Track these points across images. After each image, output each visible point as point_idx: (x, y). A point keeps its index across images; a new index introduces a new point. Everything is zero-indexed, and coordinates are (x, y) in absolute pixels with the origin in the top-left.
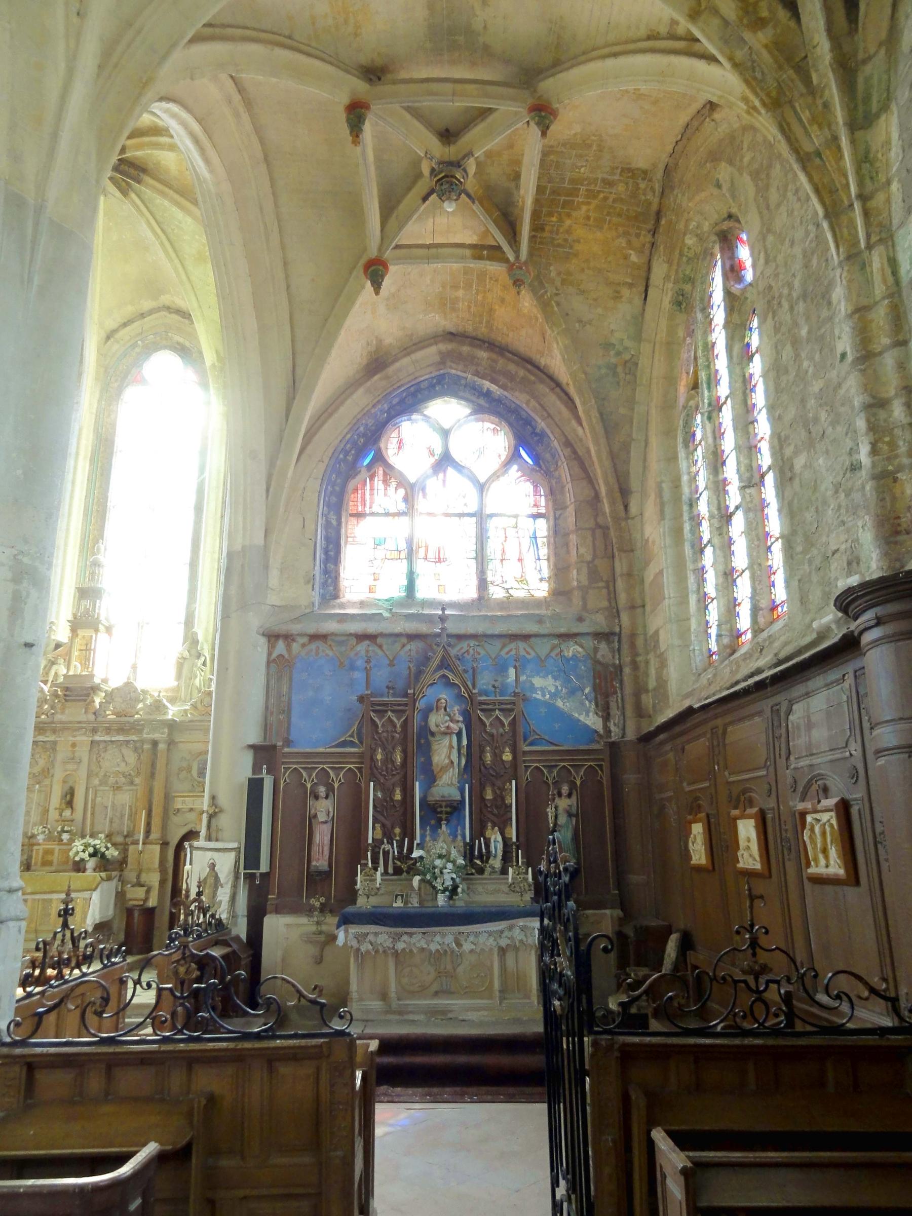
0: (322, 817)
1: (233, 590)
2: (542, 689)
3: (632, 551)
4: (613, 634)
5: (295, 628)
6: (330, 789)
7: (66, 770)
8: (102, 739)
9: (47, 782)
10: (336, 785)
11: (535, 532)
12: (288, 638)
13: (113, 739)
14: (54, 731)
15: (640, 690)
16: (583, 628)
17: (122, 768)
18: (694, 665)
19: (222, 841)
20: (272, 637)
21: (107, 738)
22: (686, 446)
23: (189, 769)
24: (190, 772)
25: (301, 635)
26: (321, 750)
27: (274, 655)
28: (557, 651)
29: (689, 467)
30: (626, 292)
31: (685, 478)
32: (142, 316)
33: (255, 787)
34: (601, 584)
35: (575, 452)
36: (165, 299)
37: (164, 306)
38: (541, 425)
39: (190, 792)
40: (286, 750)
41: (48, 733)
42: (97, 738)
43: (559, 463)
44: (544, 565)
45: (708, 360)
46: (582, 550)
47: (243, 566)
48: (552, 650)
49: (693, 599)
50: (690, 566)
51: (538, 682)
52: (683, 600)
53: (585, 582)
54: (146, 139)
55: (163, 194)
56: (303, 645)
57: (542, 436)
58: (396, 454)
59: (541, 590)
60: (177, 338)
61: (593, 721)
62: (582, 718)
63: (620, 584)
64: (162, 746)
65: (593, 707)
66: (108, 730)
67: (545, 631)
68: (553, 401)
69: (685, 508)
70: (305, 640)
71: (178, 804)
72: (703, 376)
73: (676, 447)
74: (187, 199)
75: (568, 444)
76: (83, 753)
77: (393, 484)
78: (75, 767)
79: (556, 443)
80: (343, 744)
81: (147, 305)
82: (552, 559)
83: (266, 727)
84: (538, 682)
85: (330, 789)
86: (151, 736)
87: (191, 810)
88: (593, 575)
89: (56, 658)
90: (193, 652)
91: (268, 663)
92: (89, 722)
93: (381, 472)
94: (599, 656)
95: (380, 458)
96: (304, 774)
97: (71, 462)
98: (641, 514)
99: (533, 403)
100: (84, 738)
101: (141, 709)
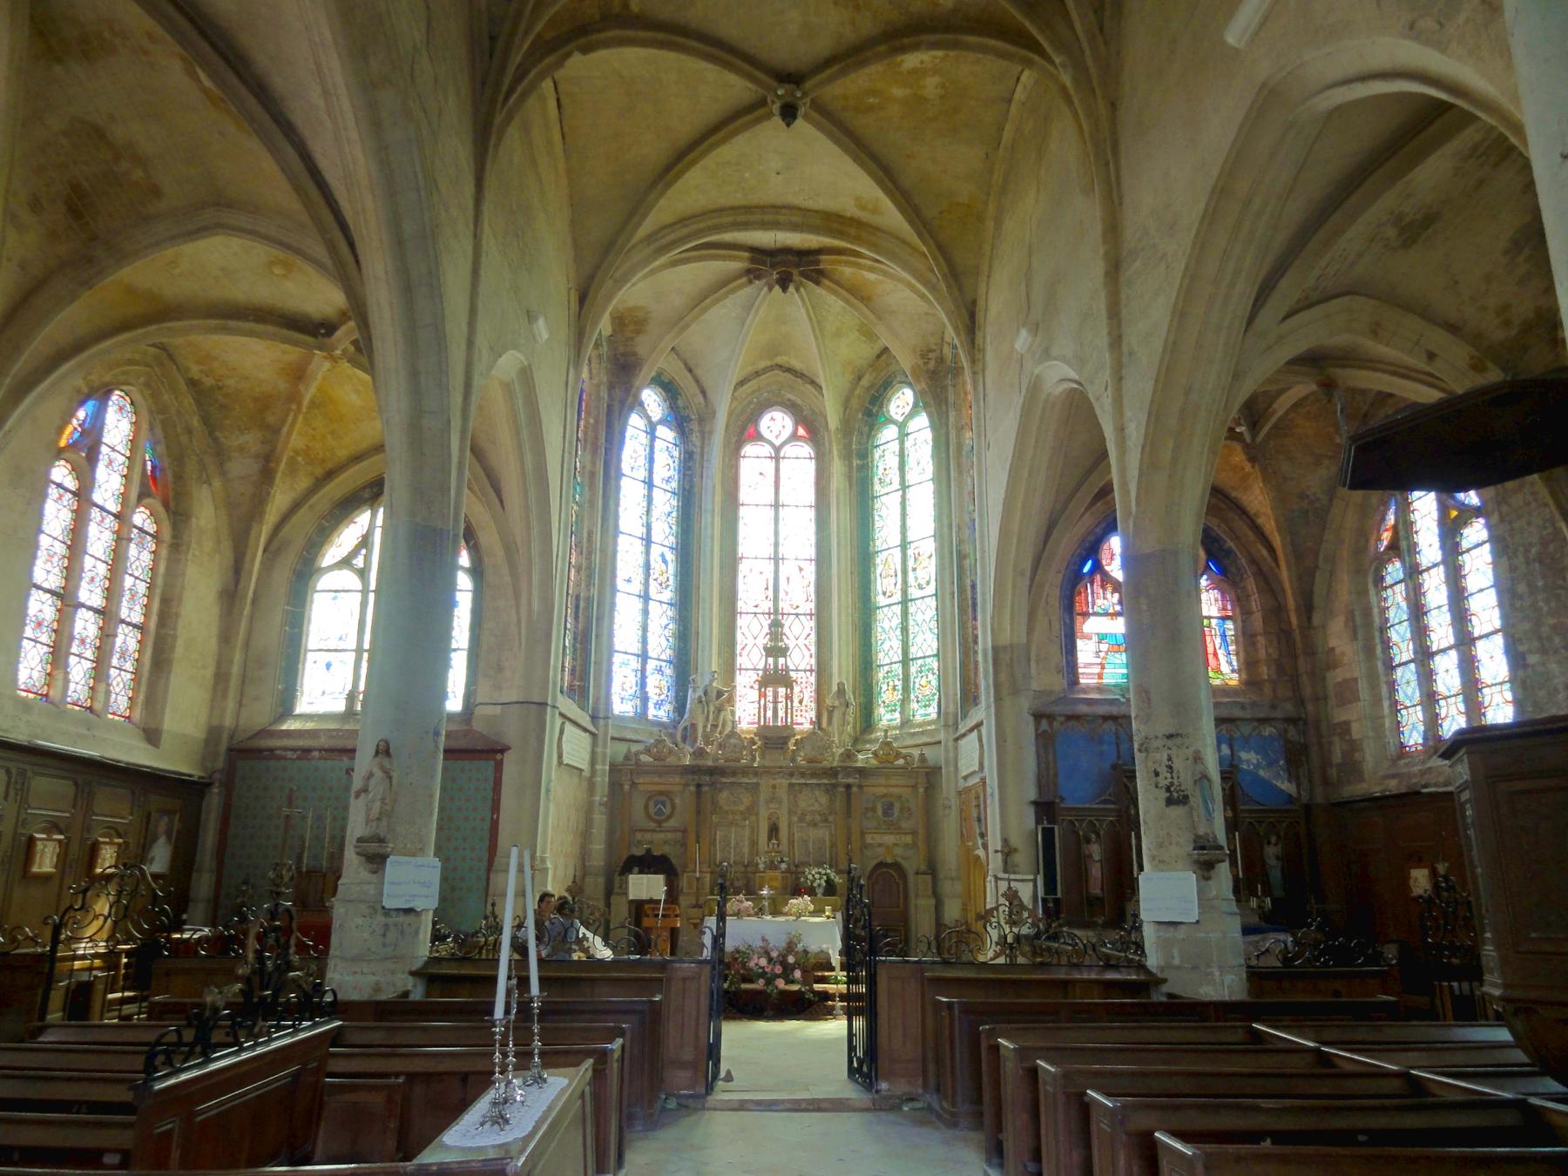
0: (1097, 857)
1: (1003, 676)
2: (1248, 761)
3: (1314, 654)
4: (1300, 719)
5: (1057, 709)
6: (1098, 835)
7: (769, 809)
9: (753, 818)
10: (1102, 833)
11: (1224, 631)
12: (1051, 717)
14: (756, 774)
15: (1326, 764)
16: (1278, 714)
17: (817, 807)
18: (1388, 753)
19: (1019, 873)
20: (1038, 717)
21: (802, 781)
22: (1376, 586)
23: (874, 810)
24: (875, 812)
25: (1060, 715)
26: (1087, 806)
27: (1040, 731)
28: (1257, 731)
29: (1379, 602)
30: (1326, 462)
31: (1376, 610)
32: (757, 374)
33: (1048, 835)
34: (1286, 678)
35: (1260, 569)
36: (779, 360)
37: (777, 365)
38: (1231, 544)
39: (876, 828)
40: (1062, 805)
41: (751, 776)
42: (794, 781)
43: (1245, 576)
44: (1234, 658)
45: (1407, 532)
46: (1270, 650)
47: (1011, 659)
48: (1254, 729)
49: (1386, 704)
50: (1383, 679)
51: (1244, 755)
52: (1377, 701)
53: (1275, 677)
54: (844, 258)
55: (835, 293)
56: (1062, 723)
57: (1229, 552)
58: (1109, 564)
59: (1234, 680)
60: (790, 396)
61: (1286, 786)
62: (1279, 784)
63: (1305, 679)
64: (854, 789)
65: (1286, 776)
66: (803, 775)
67: (1249, 716)
68: (1240, 525)
69: (1377, 634)
70: (1062, 719)
71: (869, 840)
72: (1403, 544)
73: (1366, 584)
74: (856, 298)
75: (1253, 561)
76: (783, 794)
77: (1109, 590)
78: (777, 806)
79: (1243, 560)
80: (1105, 802)
81: (763, 364)
82: (1242, 655)
83: (1040, 786)
84: (1244, 755)
85: (1098, 835)
87: (880, 845)
88: (1281, 669)
89: (722, 705)
90: (842, 700)
91: (1038, 736)
92: (788, 767)
93: (1098, 577)
94: (1289, 735)
95: (1098, 567)
96: (1077, 824)
97: (706, 518)
98: (1324, 626)
99: (1223, 526)
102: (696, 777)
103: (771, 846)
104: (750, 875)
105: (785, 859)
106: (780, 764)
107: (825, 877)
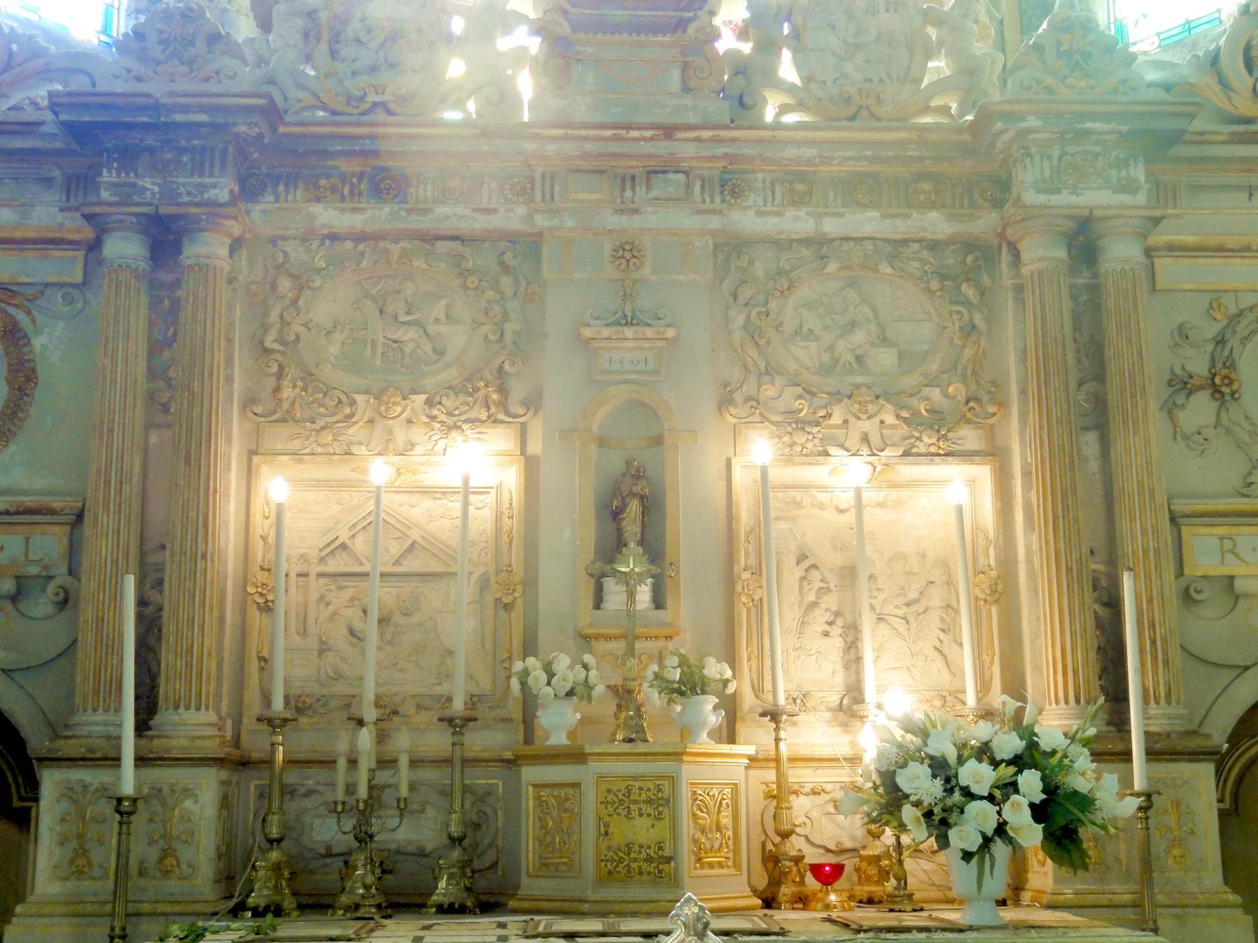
8: (768, 225)
13: (831, 227)
21: (798, 222)
86: (1065, 199)
100: (684, 219)
101: (940, 86)
102: (150, 185)
103: (615, 595)
104: (480, 779)
105: (715, 669)
106: (662, 116)
107: (1030, 782)
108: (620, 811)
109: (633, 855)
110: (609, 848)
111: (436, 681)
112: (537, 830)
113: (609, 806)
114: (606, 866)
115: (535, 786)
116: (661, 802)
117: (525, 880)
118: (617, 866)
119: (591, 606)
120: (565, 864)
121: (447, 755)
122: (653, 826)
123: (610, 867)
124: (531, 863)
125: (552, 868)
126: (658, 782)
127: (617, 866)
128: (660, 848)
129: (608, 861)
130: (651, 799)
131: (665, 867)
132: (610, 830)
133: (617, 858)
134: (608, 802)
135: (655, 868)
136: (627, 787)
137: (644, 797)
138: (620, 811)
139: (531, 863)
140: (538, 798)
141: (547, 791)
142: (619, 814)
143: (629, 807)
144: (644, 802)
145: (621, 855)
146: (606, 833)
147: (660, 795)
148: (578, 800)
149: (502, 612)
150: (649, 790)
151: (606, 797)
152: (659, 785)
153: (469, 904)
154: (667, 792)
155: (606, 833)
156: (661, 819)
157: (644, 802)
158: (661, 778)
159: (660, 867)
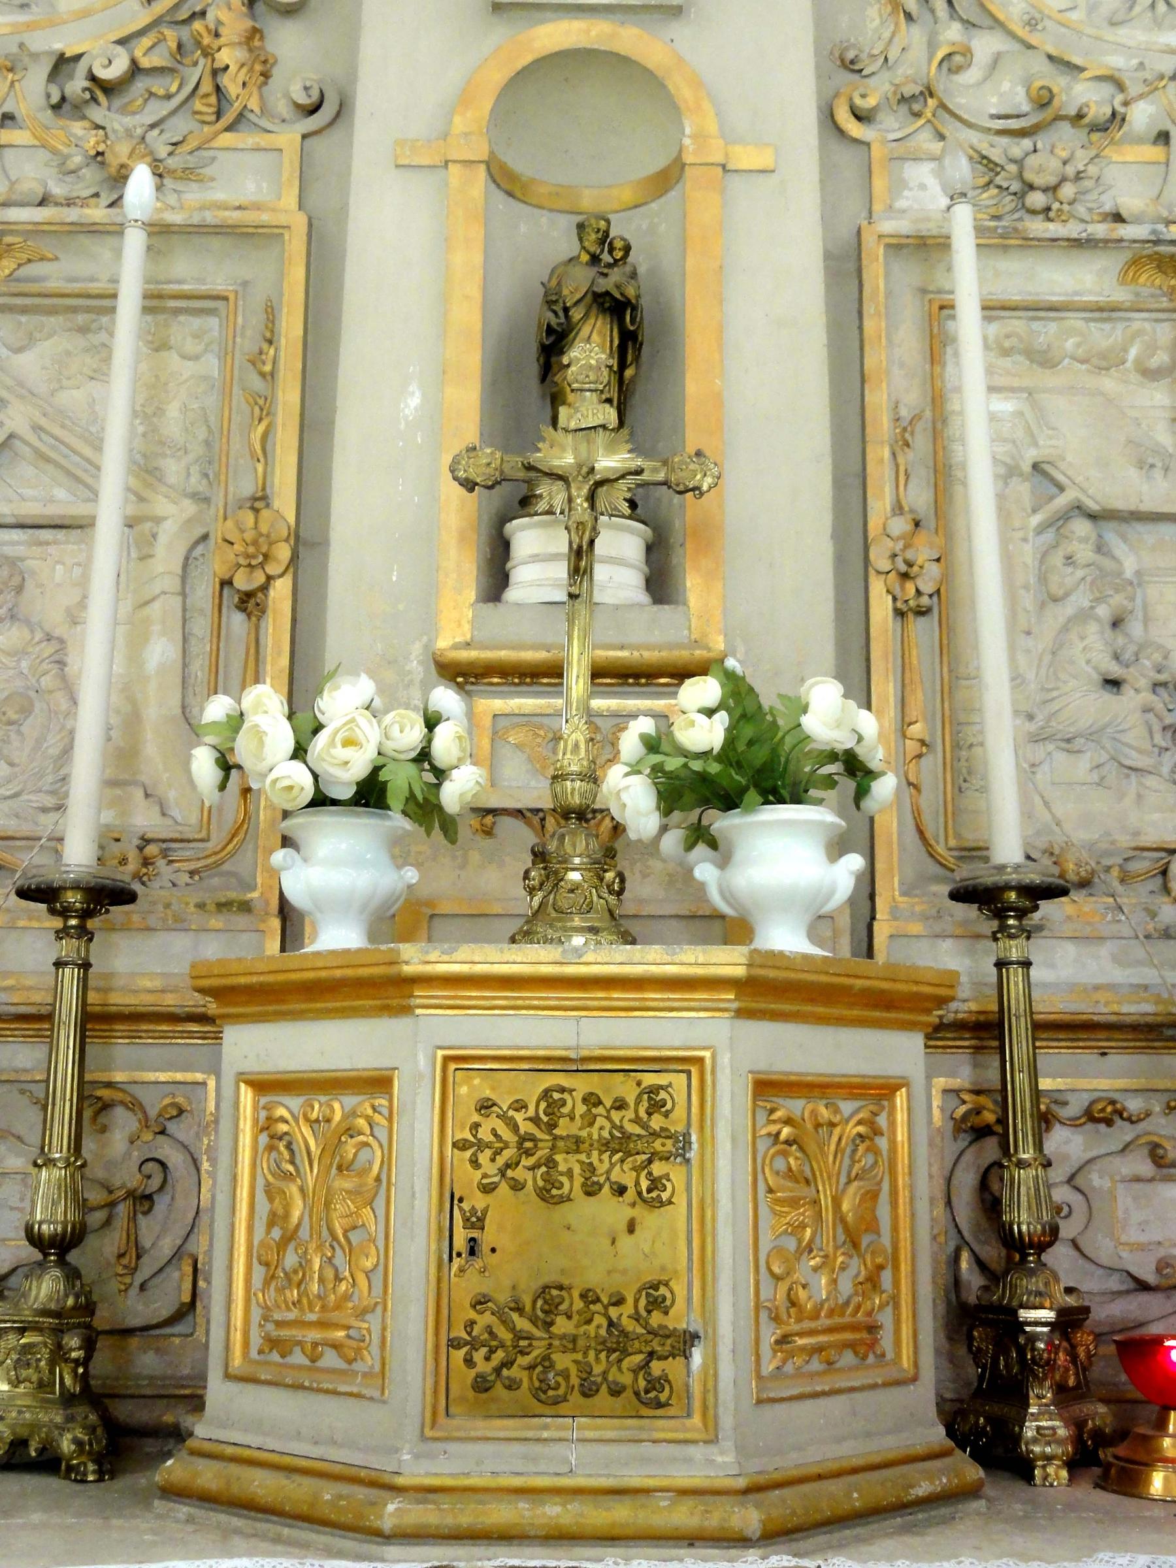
108: (519, 1173)
109: (562, 1326)
110: (480, 1302)
111: (50, 801)
112: (259, 1233)
113: (484, 1158)
114: (469, 1362)
115: (263, 1086)
116: (657, 1145)
117: (217, 1391)
118: (507, 1364)
119: (471, 594)
120: (336, 1346)
121: (40, 998)
122: (631, 1228)
123: (483, 1367)
124: (237, 1337)
125: (298, 1358)
126: (649, 1079)
127: (507, 1364)
128: (657, 1304)
129: (474, 1344)
130: (627, 1137)
131: (671, 1367)
132: (487, 1238)
133: (505, 1335)
134: (481, 1145)
135: (635, 1372)
136: (546, 1094)
137: (601, 1129)
138: (519, 1173)
139: (237, 1337)
140: (266, 1125)
141: (295, 1102)
142: (517, 1186)
143: (550, 1163)
144: (606, 1146)
145: (522, 1324)
146: (473, 1249)
147: (657, 1122)
148: (382, 1134)
149: (238, 618)
150: (620, 1105)
151: (476, 1126)
152: (653, 1090)
153: (66, 1445)
154: (679, 1113)
155: (473, 1249)
156: (662, 1204)
157: (606, 1146)
158: (662, 1063)
159: (656, 1367)
